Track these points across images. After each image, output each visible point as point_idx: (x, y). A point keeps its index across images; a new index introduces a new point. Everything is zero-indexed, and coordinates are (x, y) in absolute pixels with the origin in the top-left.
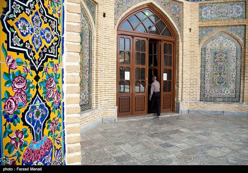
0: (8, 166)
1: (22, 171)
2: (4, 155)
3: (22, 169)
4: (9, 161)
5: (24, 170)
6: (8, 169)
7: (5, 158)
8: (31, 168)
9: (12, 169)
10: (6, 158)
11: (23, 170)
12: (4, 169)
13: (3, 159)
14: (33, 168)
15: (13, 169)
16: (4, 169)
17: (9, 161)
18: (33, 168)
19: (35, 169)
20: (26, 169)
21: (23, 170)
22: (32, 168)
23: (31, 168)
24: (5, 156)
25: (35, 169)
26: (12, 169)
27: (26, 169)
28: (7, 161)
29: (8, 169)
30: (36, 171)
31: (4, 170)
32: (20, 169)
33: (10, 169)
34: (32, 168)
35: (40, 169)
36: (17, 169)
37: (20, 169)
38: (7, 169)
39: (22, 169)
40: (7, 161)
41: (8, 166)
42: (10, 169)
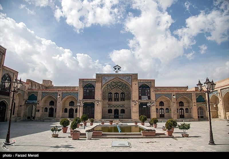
1: (20, 157)
2: (3, 142)
3: (21, 156)
4: (8, 148)
5: (22, 156)
6: (8, 156)
8: (28, 154)
9: (11, 156)
11: (21, 156)
12: (4, 156)
14: (30, 154)
15: (12, 156)
16: (4, 156)
17: (8, 148)
18: (30, 154)
19: (32, 156)
20: (24, 156)
21: (21, 156)
22: (29, 155)
23: (28, 154)
25: (32, 156)
26: (11, 156)
27: (24, 156)
29: (8, 156)
30: (34, 157)
31: (3, 156)
32: (19, 156)
33: (9, 156)
34: (29, 155)
35: (37, 156)
36: (16, 155)
37: (19, 156)
38: (7, 156)
39: (21, 156)
42: (9, 156)
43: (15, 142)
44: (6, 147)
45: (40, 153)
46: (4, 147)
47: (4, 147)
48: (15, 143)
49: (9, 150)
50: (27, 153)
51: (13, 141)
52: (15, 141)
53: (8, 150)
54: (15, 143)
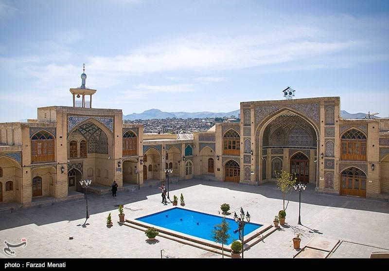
0: (12, 261)
1: (34, 268)
2: (6, 242)
3: (35, 265)
4: (14, 253)
5: (38, 266)
6: (13, 265)
8: (48, 263)
9: (18, 265)
10: (10, 248)
11: (36, 266)
12: (6, 265)
13: (6, 249)
14: (51, 263)
15: (21, 265)
16: (7, 265)
18: (51, 263)
19: (54, 265)
20: (40, 265)
21: (36, 266)
22: (50, 263)
23: (48, 263)
24: (8, 244)
25: (54, 265)
26: (18, 265)
27: (40, 265)
28: (12, 253)
29: (13, 265)
30: (57, 268)
31: (6, 267)
32: (32, 265)
33: (16, 265)
34: (50, 263)
36: (27, 265)
37: (32, 265)
38: (11, 265)
39: (35, 265)
40: (12, 253)
42: (16, 265)
43: (26, 242)
44: (9, 251)
45: (68, 261)
47: (7, 251)
48: (25, 243)
50: (46, 261)
51: (23, 240)
52: (25, 240)
53: (14, 256)
54: (25, 243)
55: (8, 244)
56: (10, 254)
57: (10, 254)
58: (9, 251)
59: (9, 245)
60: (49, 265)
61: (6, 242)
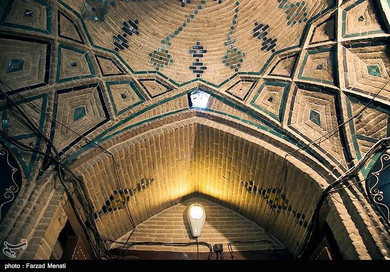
1: (34, 269)
2: (6, 243)
3: (35, 266)
4: (14, 254)
5: (38, 267)
6: (13, 266)
7: (8, 248)
8: (48, 264)
9: (18, 266)
11: (36, 267)
12: (6, 266)
13: (5, 250)
14: (51, 264)
15: (21, 266)
16: (7, 266)
18: (51, 264)
19: (54, 266)
20: (40, 266)
21: (36, 267)
22: (50, 264)
23: (48, 264)
24: (8, 245)
25: (54, 266)
26: (18, 266)
27: (40, 266)
28: (12, 254)
29: (13, 266)
31: (6, 268)
32: (32, 266)
33: (16, 266)
34: (50, 264)
36: (27, 266)
37: (32, 266)
38: (12, 266)
39: (35, 266)
40: (12, 254)
41: (13, 262)
42: (16, 266)
43: (26, 243)
44: (10, 252)
46: (6, 252)
47: (6, 252)
48: (25, 244)
49: (16, 257)
51: (23, 241)
53: (14, 256)
54: (25, 244)
55: (8, 245)
56: (11, 255)
57: (11, 255)
58: (10, 252)
59: (9, 246)
60: (50, 266)
61: (6, 243)
